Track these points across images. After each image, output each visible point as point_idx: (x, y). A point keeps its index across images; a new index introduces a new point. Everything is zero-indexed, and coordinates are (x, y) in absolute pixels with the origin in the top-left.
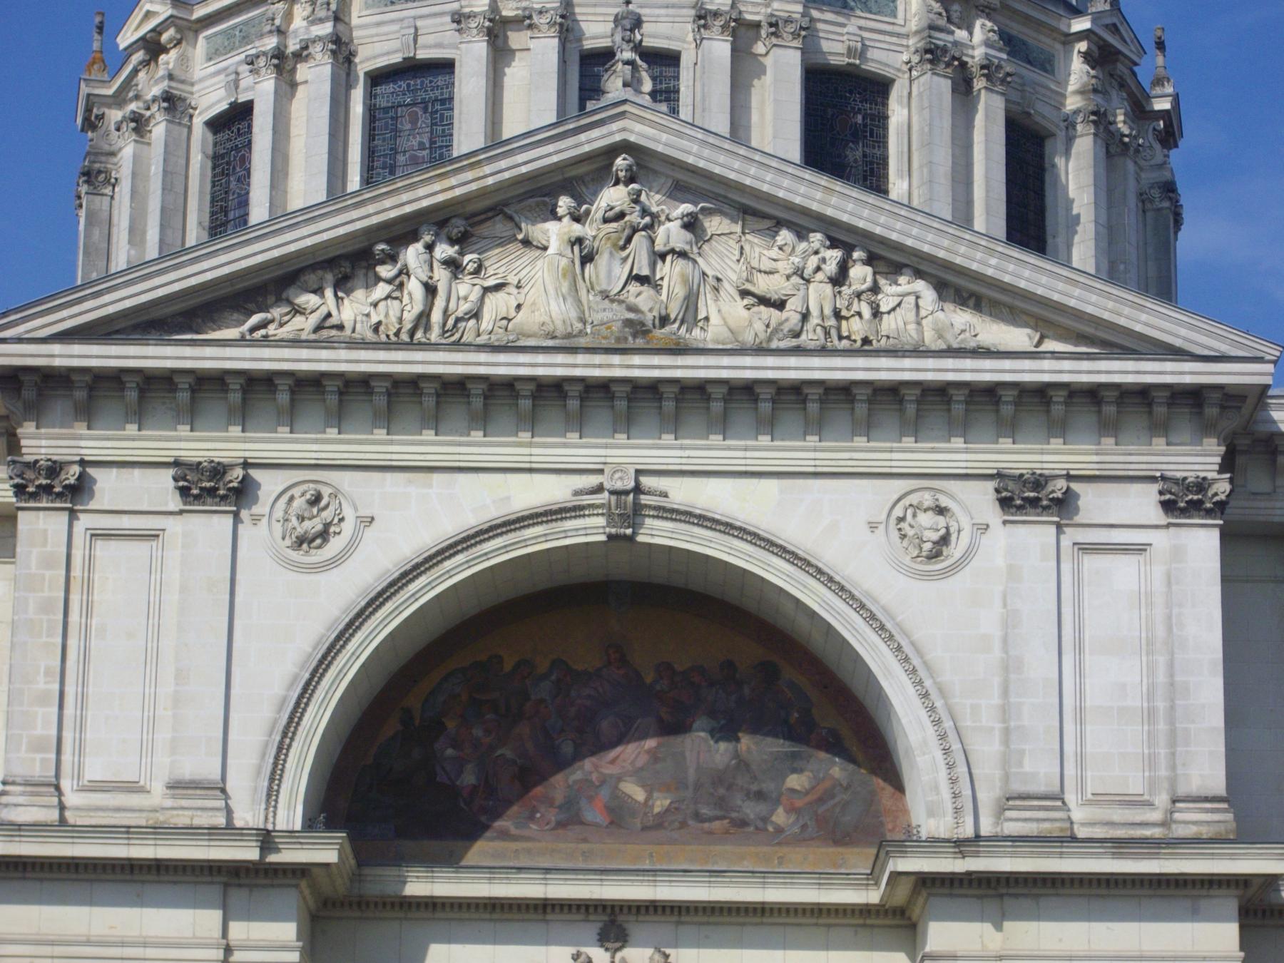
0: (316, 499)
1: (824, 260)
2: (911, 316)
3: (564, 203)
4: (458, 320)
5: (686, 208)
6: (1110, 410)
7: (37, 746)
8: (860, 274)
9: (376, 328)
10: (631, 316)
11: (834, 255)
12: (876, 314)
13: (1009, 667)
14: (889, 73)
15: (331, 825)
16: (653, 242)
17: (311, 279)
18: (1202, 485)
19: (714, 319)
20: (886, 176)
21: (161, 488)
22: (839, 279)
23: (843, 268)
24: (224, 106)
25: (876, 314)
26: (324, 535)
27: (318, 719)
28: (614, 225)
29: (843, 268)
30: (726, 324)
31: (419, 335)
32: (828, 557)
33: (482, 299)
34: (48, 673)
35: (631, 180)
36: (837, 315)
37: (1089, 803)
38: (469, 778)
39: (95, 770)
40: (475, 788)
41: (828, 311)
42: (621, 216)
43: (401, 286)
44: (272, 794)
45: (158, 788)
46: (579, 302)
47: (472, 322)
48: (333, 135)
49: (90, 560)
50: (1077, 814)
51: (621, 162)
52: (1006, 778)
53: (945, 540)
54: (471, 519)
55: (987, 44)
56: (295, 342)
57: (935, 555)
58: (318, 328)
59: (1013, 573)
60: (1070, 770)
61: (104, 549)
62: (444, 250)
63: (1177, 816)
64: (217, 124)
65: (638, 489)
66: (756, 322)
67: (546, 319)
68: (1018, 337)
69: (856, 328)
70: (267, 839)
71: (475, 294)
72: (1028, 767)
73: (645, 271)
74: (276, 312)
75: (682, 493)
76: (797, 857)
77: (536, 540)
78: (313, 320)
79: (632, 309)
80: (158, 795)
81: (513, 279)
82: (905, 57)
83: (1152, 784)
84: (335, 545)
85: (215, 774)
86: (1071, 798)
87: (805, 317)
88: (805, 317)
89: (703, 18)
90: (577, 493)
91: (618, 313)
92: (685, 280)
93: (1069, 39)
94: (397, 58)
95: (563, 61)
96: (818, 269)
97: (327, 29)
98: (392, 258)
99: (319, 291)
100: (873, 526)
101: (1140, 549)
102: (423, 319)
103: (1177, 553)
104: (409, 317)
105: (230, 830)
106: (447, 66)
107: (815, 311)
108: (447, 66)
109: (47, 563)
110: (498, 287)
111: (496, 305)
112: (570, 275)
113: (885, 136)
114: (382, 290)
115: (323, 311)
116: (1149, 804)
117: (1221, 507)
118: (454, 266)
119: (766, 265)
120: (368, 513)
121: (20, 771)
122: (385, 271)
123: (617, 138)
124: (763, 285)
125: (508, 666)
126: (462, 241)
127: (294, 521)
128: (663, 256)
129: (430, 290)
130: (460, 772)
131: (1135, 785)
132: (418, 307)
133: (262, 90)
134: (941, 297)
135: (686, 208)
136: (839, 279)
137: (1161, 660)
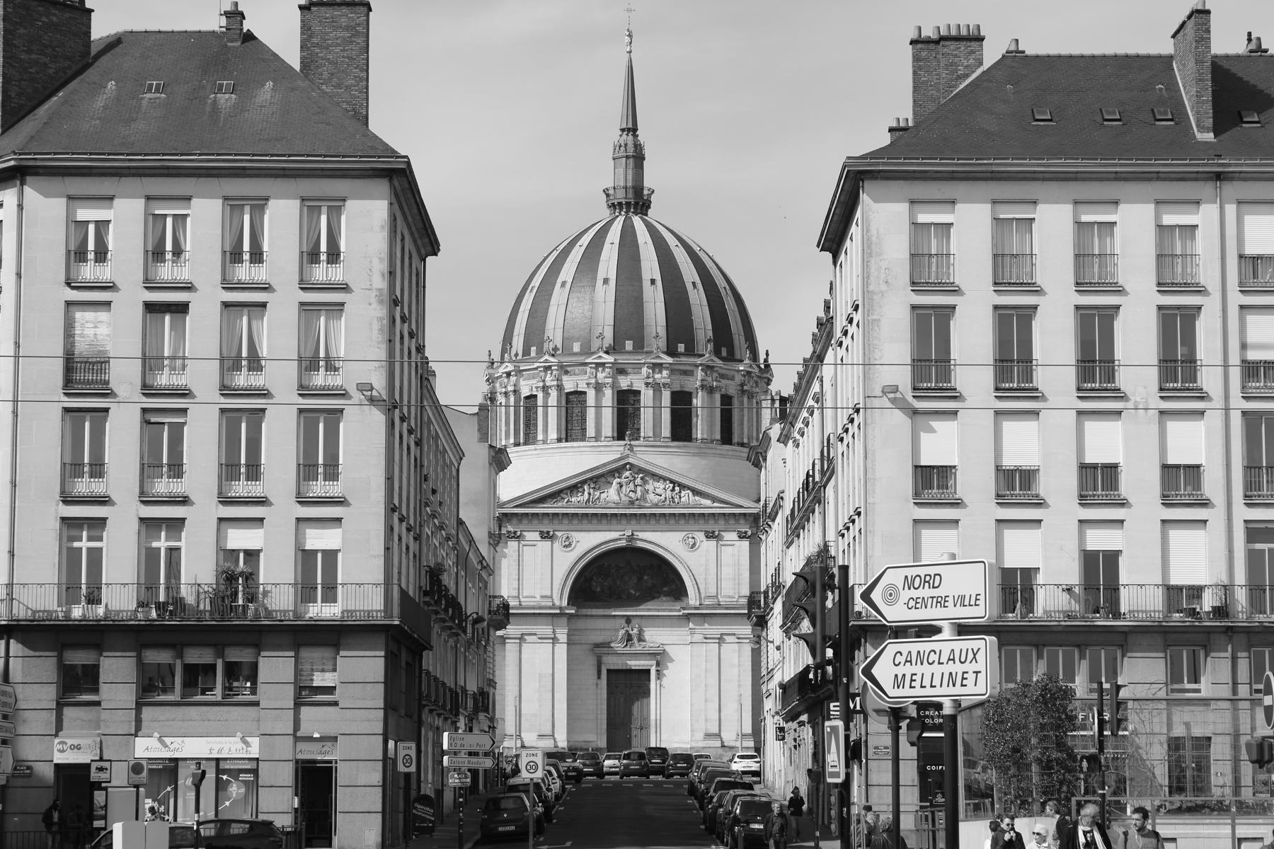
0: (568, 537)
3: (617, 475)
5: (641, 475)
6: (727, 517)
7: (515, 589)
8: (677, 489)
11: (672, 485)
12: (680, 498)
13: (707, 570)
14: (692, 391)
15: (573, 605)
17: (565, 491)
18: (746, 532)
21: (536, 536)
22: (673, 490)
23: (674, 488)
24: (529, 394)
25: (680, 498)
26: (570, 545)
27: (570, 583)
29: (674, 488)
32: (671, 548)
35: (630, 470)
38: (599, 589)
44: (561, 598)
45: (538, 597)
50: (721, 600)
51: (628, 466)
54: (599, 541)
57: (692, 548)
59: (708, 551)
62: (592, 486)
64: (527, 398)
65: (633, 534)
66: (655, 499)
68: (708, 502)
70: (560, 608)
72: (710, 590)
74: (559, 498)
75: (641, 535)
76: (666, 603)
79: (631, 498)
80: (538, 598)
83: (735, 593)
85: (549, 594)
89: (647, 384)
91: (628, 499)
93: (739, 371)
94: (572, 390)
95: (613, 394)
97: (555, 383)
99: (567, 494)
102: (589, 499)
103: (741, 546)
105: (555, 608)
106: (585, 393)
108: (585, 393)
109: (514, 551)
112: (618, 490)
114: (580, 494)
117: (749, 537)
118: (594, 488)
121: (511, 595)
122: (581, 490)
124: (658, 491)
125: (606, 565)
126: (595, 483)
129: (589, 494)
134: (694, 495)
135: (641, 475)
136: (673, 490)
137: (737, 568)
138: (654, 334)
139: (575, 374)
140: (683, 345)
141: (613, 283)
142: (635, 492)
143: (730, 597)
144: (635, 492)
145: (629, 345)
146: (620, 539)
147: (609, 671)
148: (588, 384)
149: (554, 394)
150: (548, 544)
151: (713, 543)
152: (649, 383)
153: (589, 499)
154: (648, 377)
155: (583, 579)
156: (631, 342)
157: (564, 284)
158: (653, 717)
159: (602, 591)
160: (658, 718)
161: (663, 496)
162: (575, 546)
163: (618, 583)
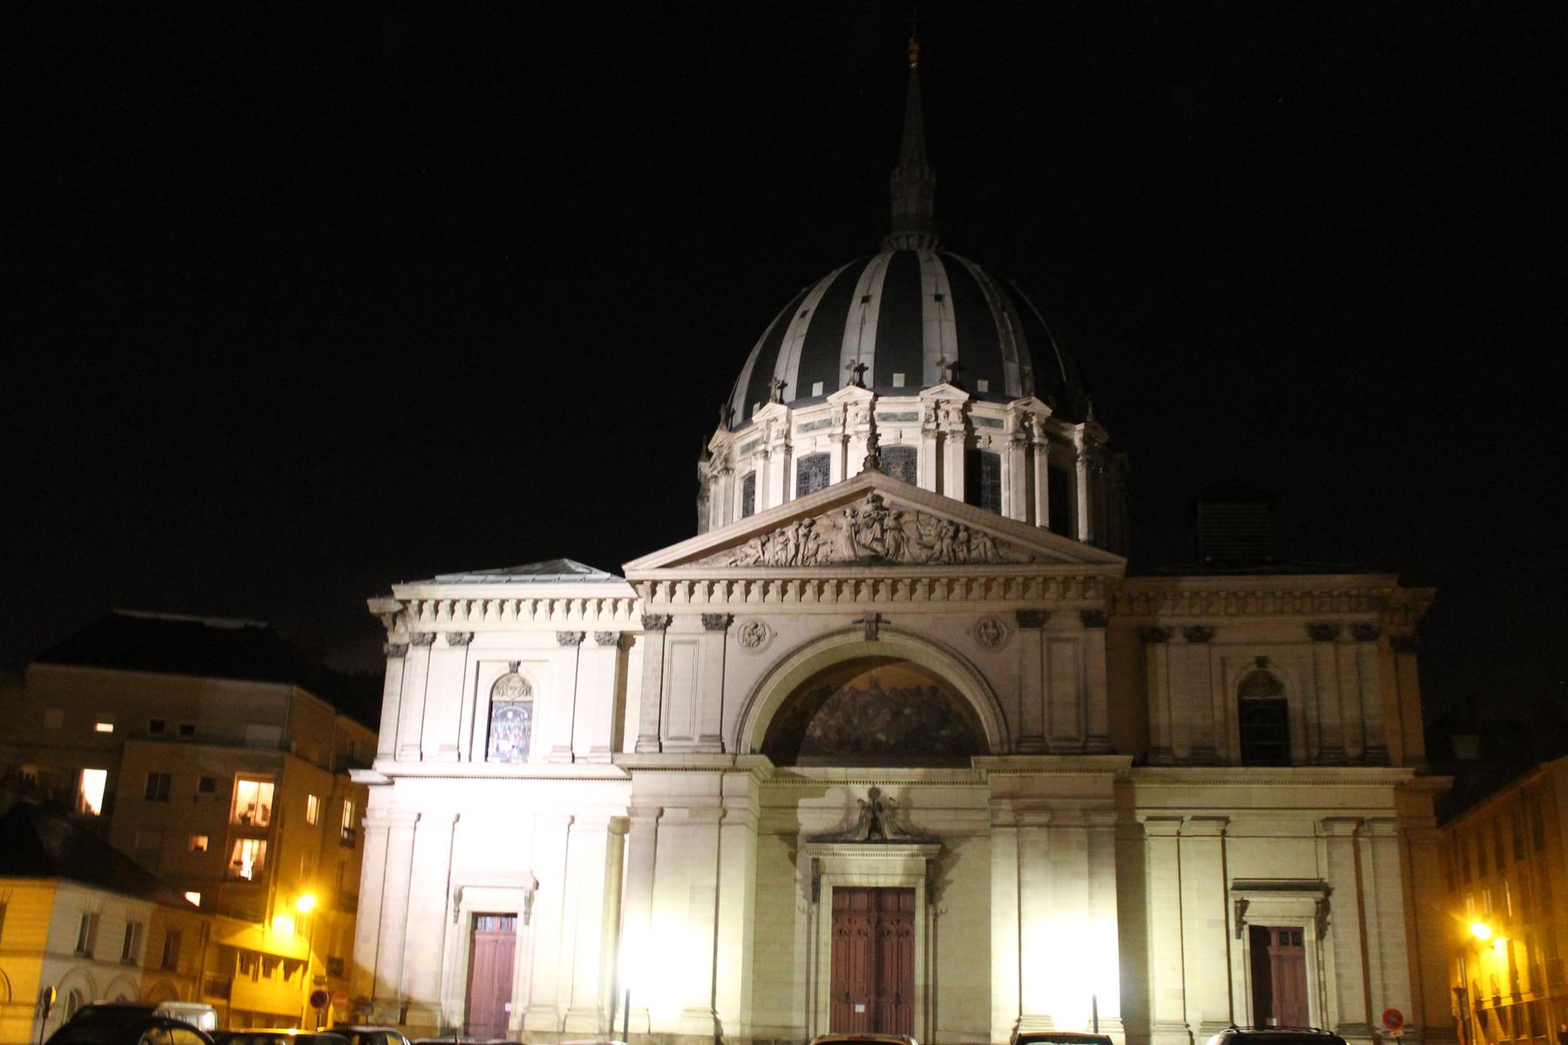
1: (948, 530)
2: (982, 551)
4: (807, 558)
9: (777, 561)
10: (873, 554)
11: (952, 530)
12: (969, 551)
13: (1021, 686)
16: (883, 526)
17: (751, 542)
19: (907, 554)
20: (1000, 490)
23: (957, 531)
25: (969, 551)
28: (867, 519)
29: (957, 531)
30: (912, 557)
31: (793, 563)
33: (818, 548)
34: (656, 695)
36: (954, 551)
37: (1052, 740)
39: (672, 733)
40: (820, 738)
41: (950, 549)
42: (870, 515)
43: (786, 545)
46: (854, 549)
47: (813, 558)
48: (784, 483)
49: (671, 653)
52: (1021, 730)
53: (998, 636)
55: (1040, 436)
56: (747, 566)
58: (755, 562)
60: (1046, 726)
61: (676, 648)
63: (1091, 744)
66: (924, 554)
67: (841, 555)
69: (961, 555)
71: (816, 546)
73: (879, 536)
77: (838, 641)
78: (753, 560)
79: (875, 551)
80: (696, 741)
81: (829, 541)
82: (1007, 444)
84: (762, 644)
86: (1046, 735)
87: (942, 551)
88: (942, 551)
89: (925, 431)
90: (854, 622)
92: (895, 540)
96: (946, 534)
98: (783, 533)
100: (968, 633)
101: (1075, 640)
102: (796, 555)
104: (790, 557)
107: (945, 550)
110: (824, 544)
111: (823, 551)
113: (999, 475)
115: (757, 556)
116: (1076, 740)
119: (927, 532)
120: (773, 631)
123: (868, 485)
127: (747, 636)
128: (886, 531)
129: (797, 547)
130: (815, 731)
131: (1073, 733)
132: (793, 553)
133: (758, 465)
138: (938, 358)
139: (813, 429)
140: (986, 383)
141: (876, 301)
142: (881, 540)
143: (1069, 739)
144: (881, 540)
145: (899, 380)
146: (855, 630)
147: (837, 891)
148: (831, 436)
149: (778, 458)
150: (716, 638)
151: (1032, 636)
152: (928, 430)
153: (796, 555)
154: (927, 421)
155: (789, 714)
156: (902, 376)
157: (804, 315)
158: (919, 980)
159: (825, 735)
160: (931, 982)
161: (937, 547)
162: (770, 643)
163: (856, 721)
